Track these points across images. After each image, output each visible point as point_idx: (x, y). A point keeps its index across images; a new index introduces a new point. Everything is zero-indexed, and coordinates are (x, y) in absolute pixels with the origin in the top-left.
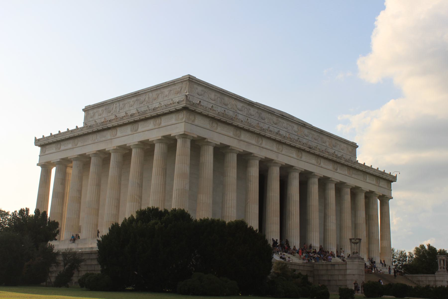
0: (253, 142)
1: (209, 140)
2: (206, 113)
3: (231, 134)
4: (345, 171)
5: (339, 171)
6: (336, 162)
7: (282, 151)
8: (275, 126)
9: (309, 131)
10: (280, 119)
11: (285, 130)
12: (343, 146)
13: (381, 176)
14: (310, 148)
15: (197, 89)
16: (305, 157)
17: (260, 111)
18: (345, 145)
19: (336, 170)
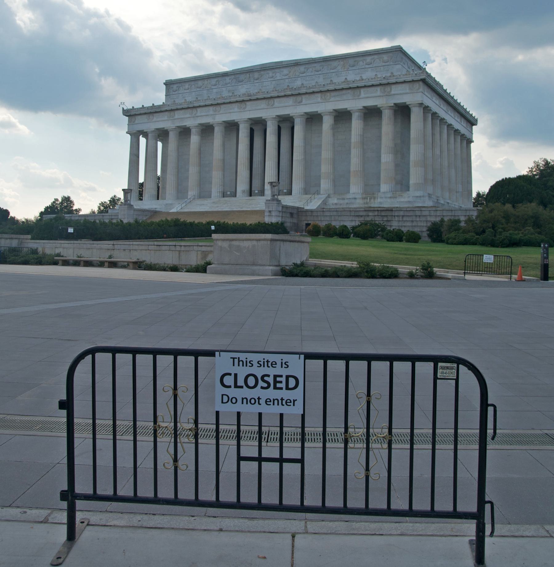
0: (188, 116)
2: (139, 112)
3: (166, 118)
5: (304, 101)
6: (297, 95)
7: (219, 112)
8: (257, 81)
9: (307, 66)
10: (262, 73)
11: (271, 79)
12: (369, 59)
13: (385, 82)
14: (249, 96)
15: (172, 88)
17: (237, 76)
18: (376, 57)
19: (301, 101)
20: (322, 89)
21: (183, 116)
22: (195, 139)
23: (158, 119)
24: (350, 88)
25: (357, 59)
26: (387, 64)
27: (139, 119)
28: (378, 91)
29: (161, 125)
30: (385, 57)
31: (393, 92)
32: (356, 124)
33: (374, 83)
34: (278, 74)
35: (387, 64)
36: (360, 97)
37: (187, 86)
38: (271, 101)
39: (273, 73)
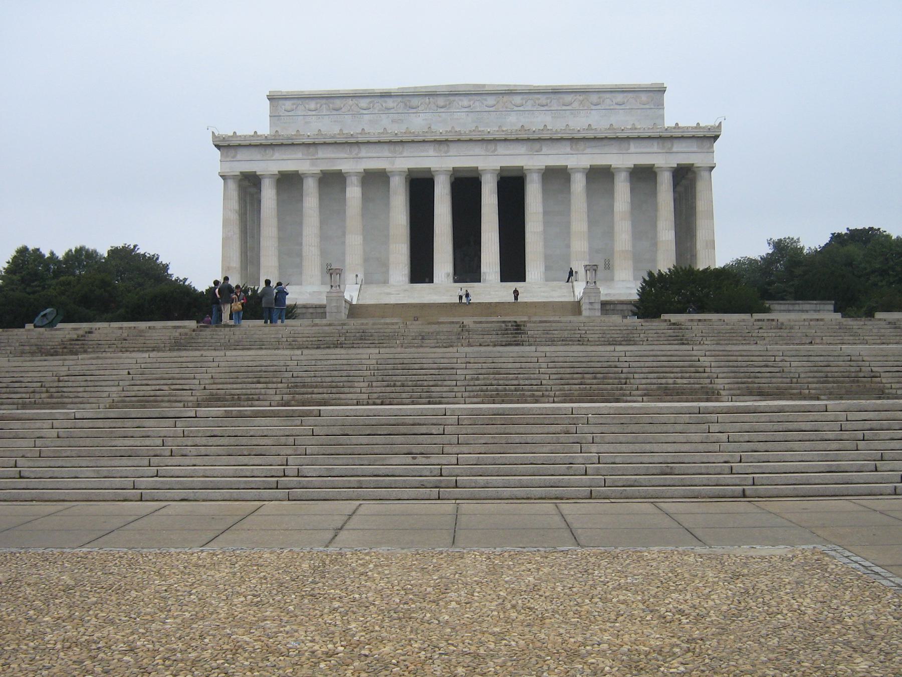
1: (258, 173)
2: (247, 143)
4: (566, 148)
7: (401, 153)
8: (443, 110)
10: (452, 98)
11: (466, 110)
12: (620, 98)
16: (454, 149)
17: (408, 98)
18: (630, 95)
20: (576, 136)
21: (333, 156)
22: (354, 192)
23: (285, 157)
24: (617, 138)
25: (601, 95)
26: (647, 107)
27: (242, 154)
28: (655, 147)
29: (290, 166)
30: (644, 97)
31: (675, 150)
32: (622, 188)
33: (652, 135)
34: (477, 104)
35: (647, 107)
36: (629, 151)
37: (312, 105)
38: (491, 147)
39: (470, 101)
